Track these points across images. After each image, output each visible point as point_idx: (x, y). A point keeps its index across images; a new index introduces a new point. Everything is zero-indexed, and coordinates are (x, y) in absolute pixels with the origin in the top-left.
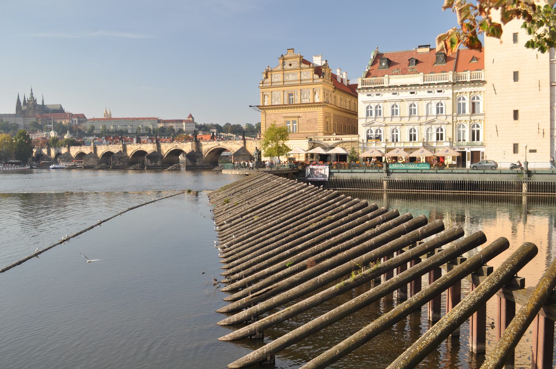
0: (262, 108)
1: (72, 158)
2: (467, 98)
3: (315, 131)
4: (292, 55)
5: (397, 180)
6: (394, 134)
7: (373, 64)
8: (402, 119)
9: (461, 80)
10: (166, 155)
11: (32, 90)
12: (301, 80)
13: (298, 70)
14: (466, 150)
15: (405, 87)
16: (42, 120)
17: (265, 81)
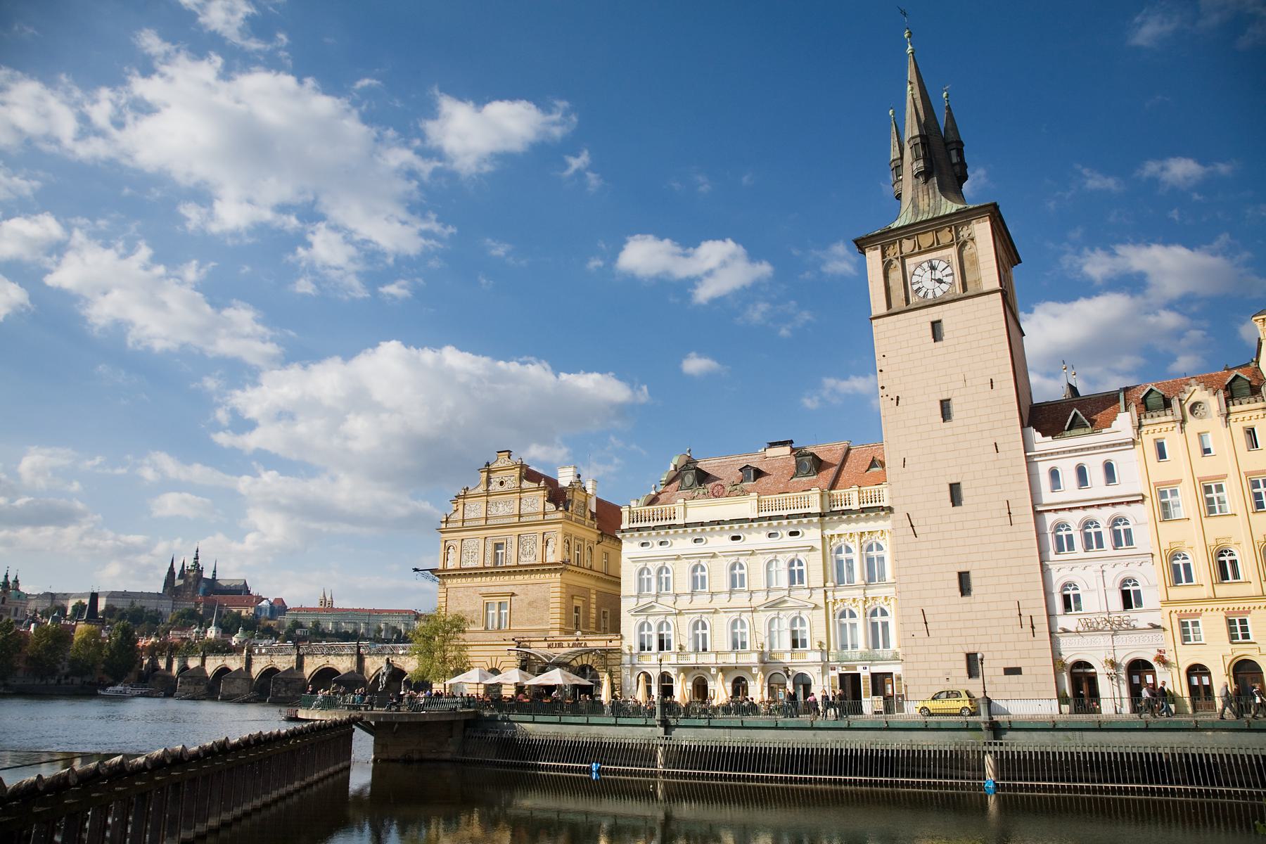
0: (441, 574)
1: (207, 677)
2: (855, 547)
3: (544, 628)
4: (506, 463)
5: (686, 746)
6: (697, 632)
7: (669, 483)
8: (714, 597)
9: (839, 508)
10: (373, 678)
11: (197, 551)
12: (520, 516)
13: (516, 494)
14: (859, 670)
15: (718, 524)
16: (205, 607)
17: (452, 517)
